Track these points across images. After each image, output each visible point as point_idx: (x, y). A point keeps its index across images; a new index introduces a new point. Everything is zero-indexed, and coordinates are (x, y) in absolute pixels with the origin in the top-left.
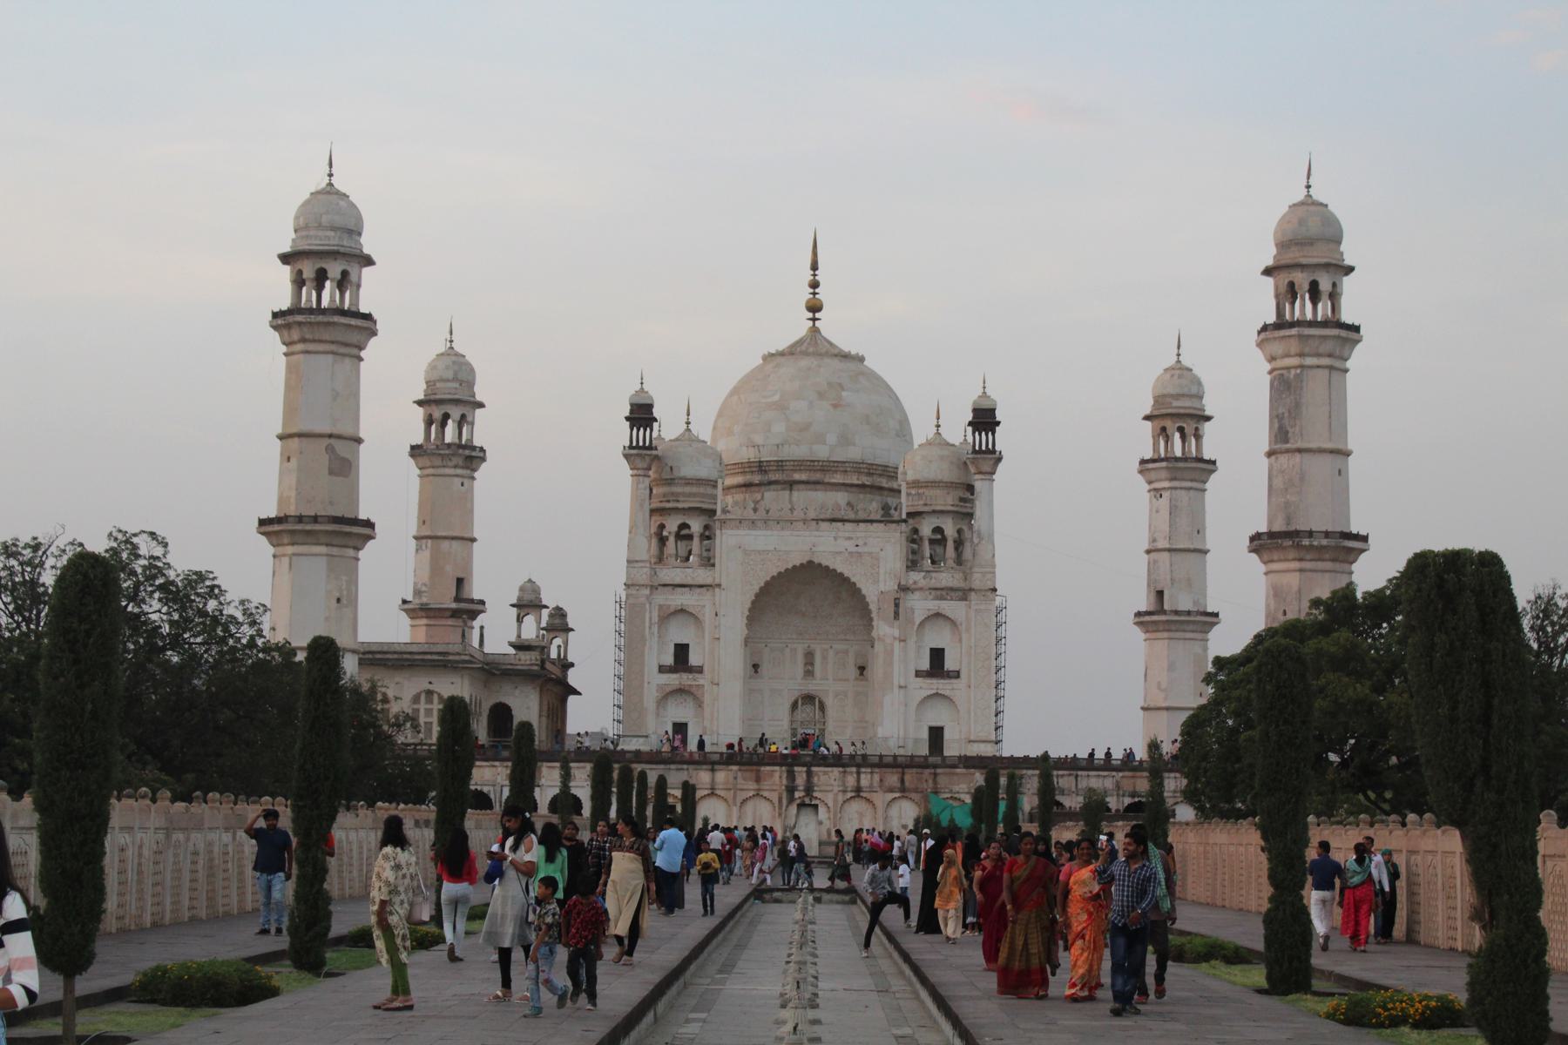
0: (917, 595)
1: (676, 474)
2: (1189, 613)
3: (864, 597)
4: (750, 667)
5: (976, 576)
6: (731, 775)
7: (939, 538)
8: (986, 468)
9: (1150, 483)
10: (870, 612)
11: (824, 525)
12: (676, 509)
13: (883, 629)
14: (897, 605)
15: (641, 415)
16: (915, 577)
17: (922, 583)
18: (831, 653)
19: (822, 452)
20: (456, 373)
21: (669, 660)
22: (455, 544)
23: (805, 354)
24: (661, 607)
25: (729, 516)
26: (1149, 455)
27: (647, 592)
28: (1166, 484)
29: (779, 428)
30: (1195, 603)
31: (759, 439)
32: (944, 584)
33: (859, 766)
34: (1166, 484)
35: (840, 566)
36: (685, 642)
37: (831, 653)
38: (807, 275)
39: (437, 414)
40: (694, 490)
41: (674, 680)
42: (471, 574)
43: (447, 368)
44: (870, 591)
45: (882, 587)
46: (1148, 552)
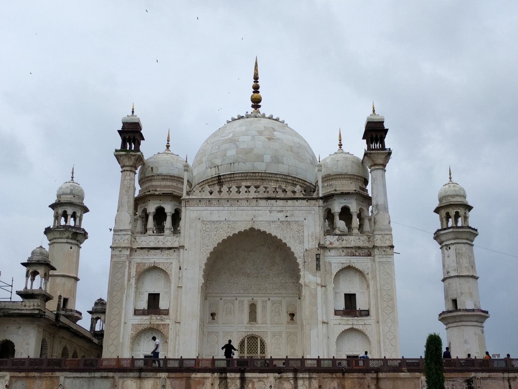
0: (333, 253)
1: (155, 172)
2: (473, 310)
3: (293, 253)
4: (208, 317)
5: (378, 237)
6: (160, 382)
7: (346, 214)
8: (380, 161)
9: (440, 244)
10: (298, 264)
11: (263, 202)
12: (153, 195)
13: (308, 277)
14: (318, 260)
15: (131, 133)
16: (330, 239)
17: (336, 244)
18: (269, 303)
19: (261, 167)
20: (71, 190)
21: (143, 305)
22: (64, 280)
23: (248, 117)
24: (138, 264)
25: (191, 197)
26: (440, 228)
27: (128, 252)
28: (453, 242)
29: (232, 153)
30: (475, 305)
31: (218, 162)
32: (353, 244)
33: (295, 371)
34: (453, 242)
35: (274, 231)
36: (156, 292)
37: (269, 303)
38: (252, 82)
39: (60, 211)
40: (169, 183)
41: (145, 320)
42: (74, 297)
43: (67, 188)
44: (297, 250)
45: (306, 247)
46: (443, 280)
